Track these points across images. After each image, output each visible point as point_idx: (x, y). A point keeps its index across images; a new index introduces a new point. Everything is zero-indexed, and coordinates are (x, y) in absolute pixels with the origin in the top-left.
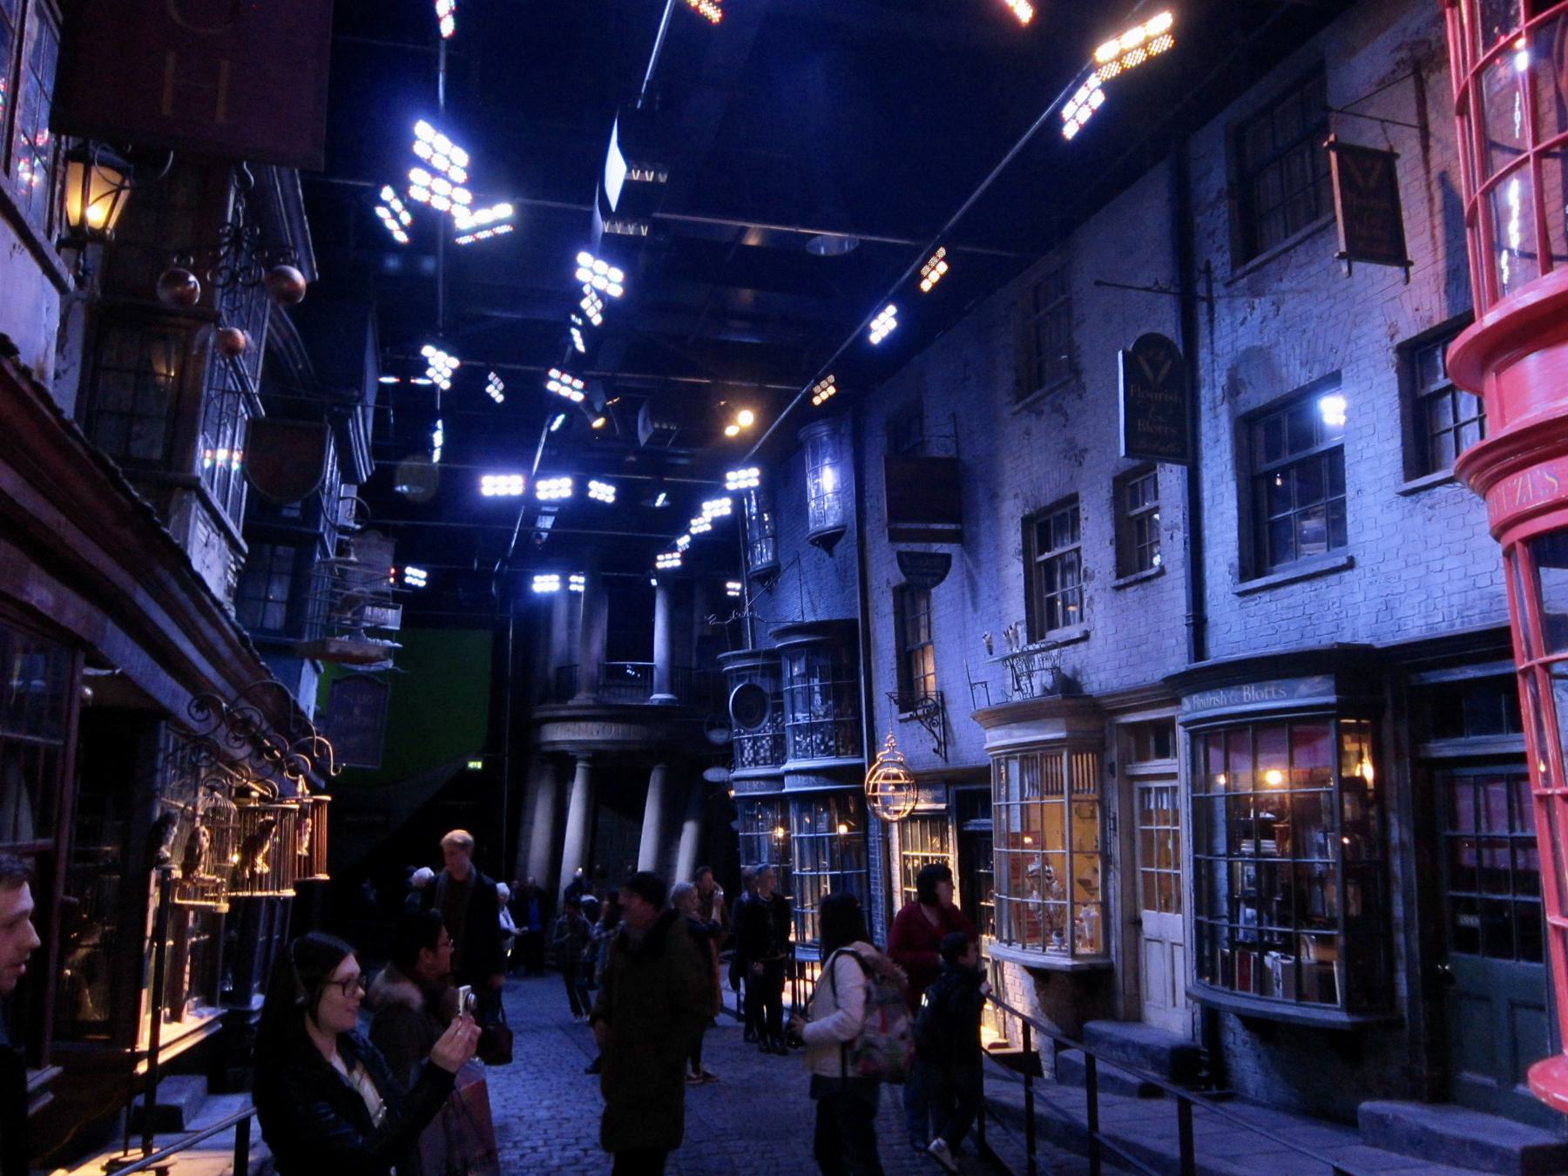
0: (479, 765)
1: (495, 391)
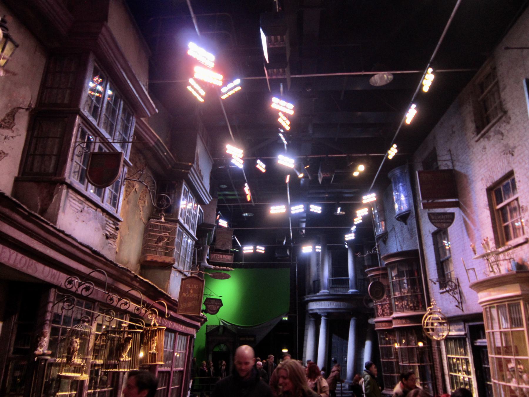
0: (287, 319)
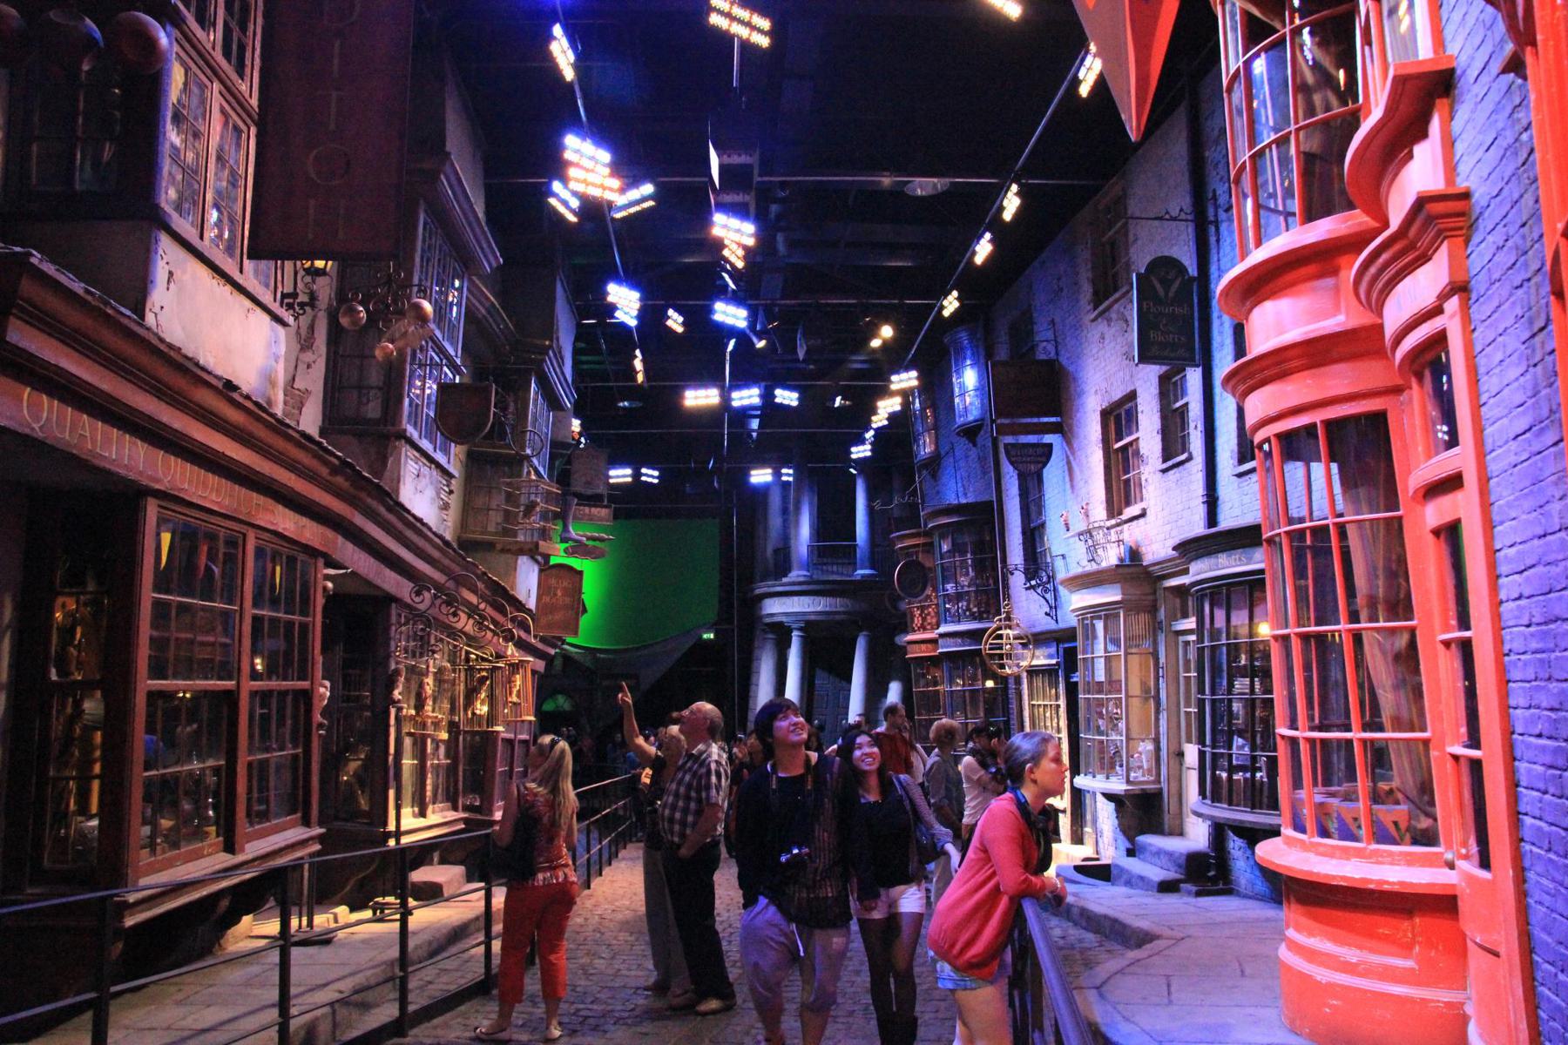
1: (675, 321)
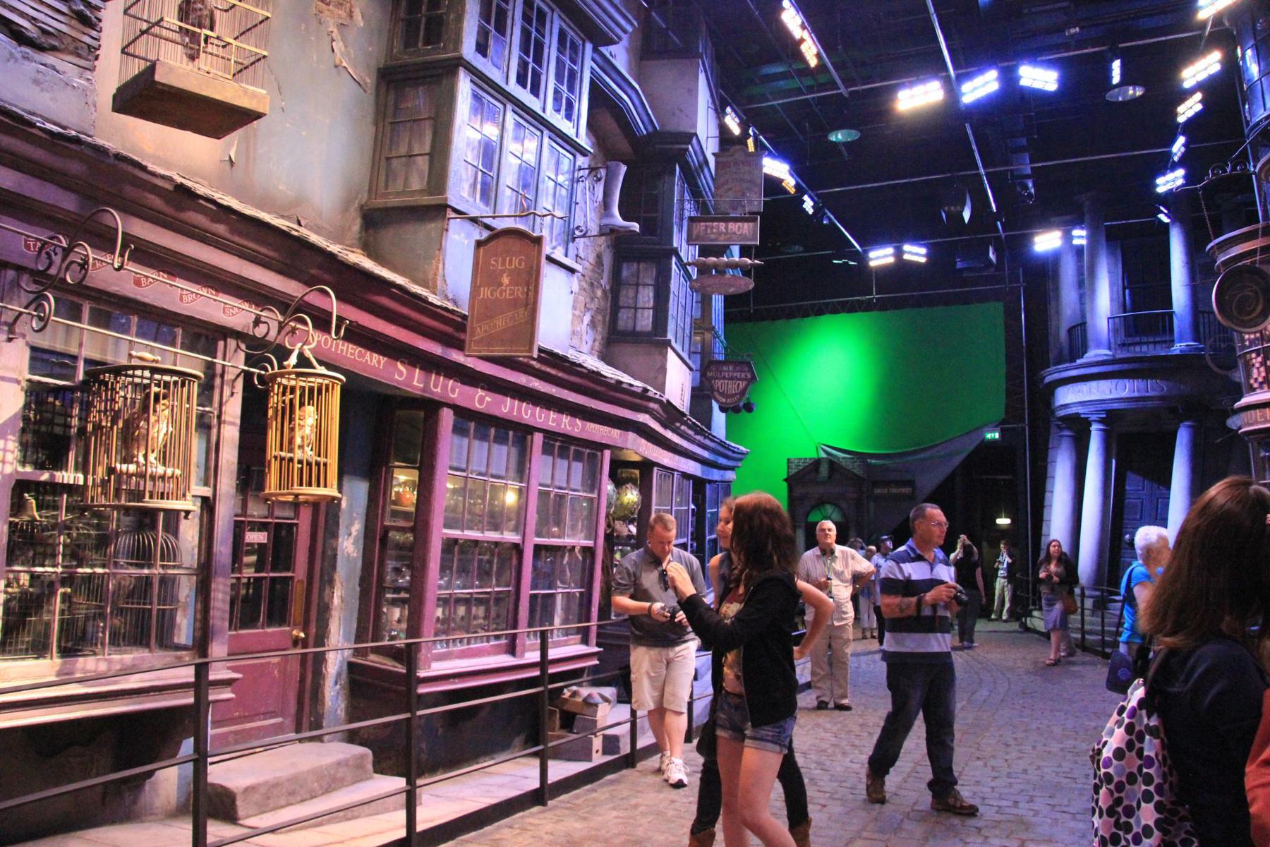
0: (997, 436)
